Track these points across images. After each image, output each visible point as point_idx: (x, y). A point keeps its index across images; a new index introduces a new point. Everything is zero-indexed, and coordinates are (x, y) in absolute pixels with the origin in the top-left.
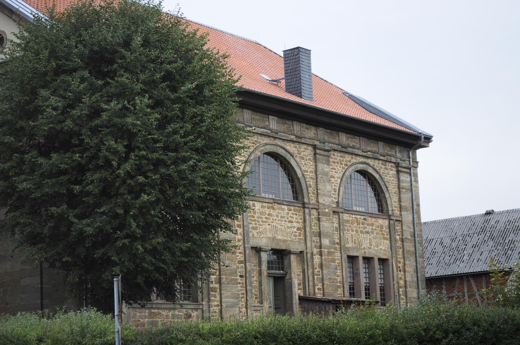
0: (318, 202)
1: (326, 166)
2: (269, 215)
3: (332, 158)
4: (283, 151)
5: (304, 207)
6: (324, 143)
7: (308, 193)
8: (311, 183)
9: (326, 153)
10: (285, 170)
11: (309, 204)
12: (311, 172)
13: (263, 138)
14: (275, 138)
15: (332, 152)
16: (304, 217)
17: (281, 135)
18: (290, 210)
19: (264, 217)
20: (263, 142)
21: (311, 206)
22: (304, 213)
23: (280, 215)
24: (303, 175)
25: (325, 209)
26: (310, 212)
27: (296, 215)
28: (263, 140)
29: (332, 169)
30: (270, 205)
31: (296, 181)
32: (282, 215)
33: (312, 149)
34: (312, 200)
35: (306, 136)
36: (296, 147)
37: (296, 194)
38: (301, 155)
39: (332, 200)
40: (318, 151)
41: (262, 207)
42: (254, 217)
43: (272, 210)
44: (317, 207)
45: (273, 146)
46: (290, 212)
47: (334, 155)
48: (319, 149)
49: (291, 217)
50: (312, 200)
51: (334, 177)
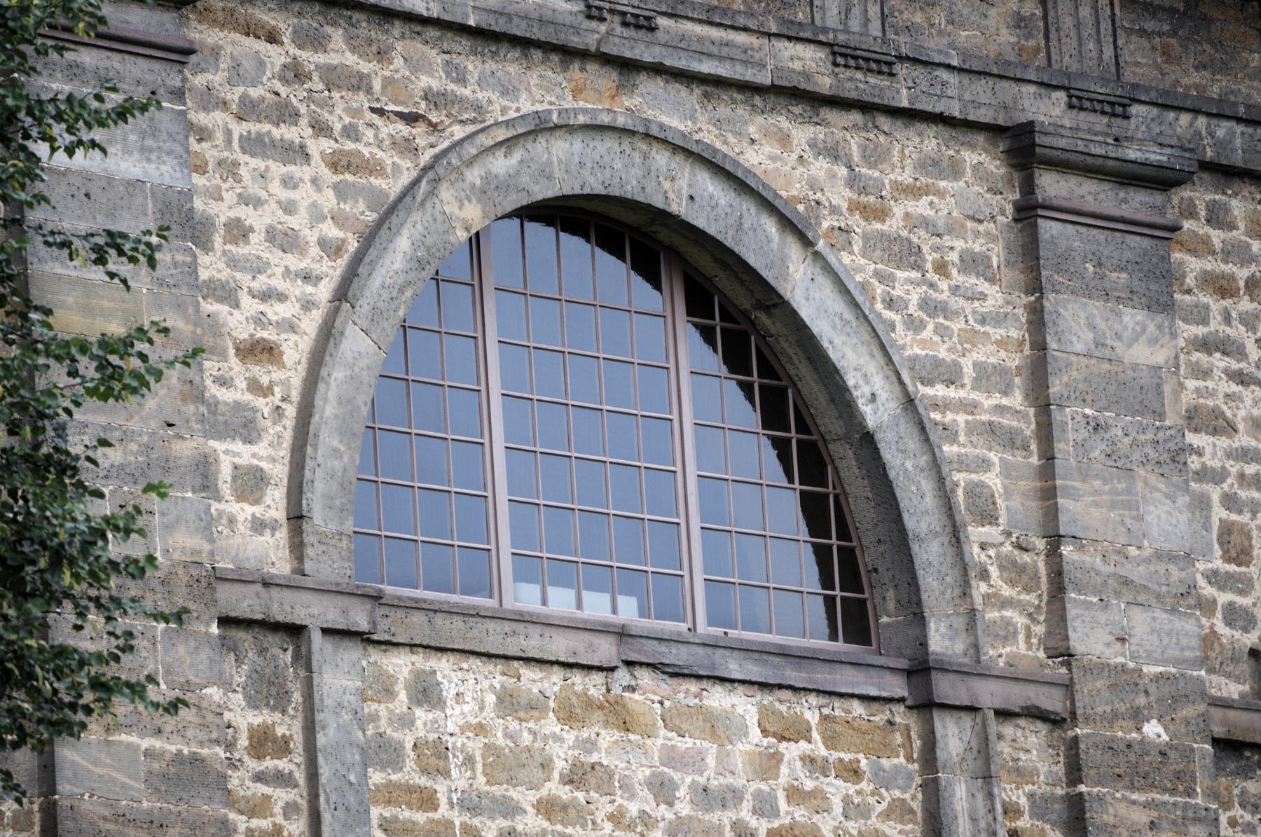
0: (1065, 655)
1: (1132, 317)
2: (574, 778)
3: (1202, 247)
4: (709, 185)
5: (926, 706)
6: (1117, 108)
7: (964, 571)
8: (994, 480)
9: (1137, 203)
10: (736, 360)
11: (977, 670)
12: (987, 377)
13: (510, 66)
14: (627, 67)
15: (1201, 195)
16: (933, 791)
17: (679, 45)
18: (794, 731)
19: (525, 797)
20: (500, 108)
21: (990, 694)
22: (929, 758)
23: (685, 782)
24: (909, 402)
25: (1138, 717)
26: (984, 748)
27: (854, 773)
28: (508, 91)
29: (1206, 345)
30: (593, 685)
31: (846, 461)
32: (711, 776)
33: (995, 166)
34: (1007, 634)
35: (934, 47)
36: (834, 153)
37: (852, 579)
38: (893, 225)
39: (1210, 639)
40: (1051, 185)
41: (509, 703)
42: (428, 801)
43: (608, 737)
44: (1052, 701)
45: (604, 147)
46: (792, 751)
47: (1217, 217)
48: (1062, 165)
49: (795, 794)
50: (1007, 634)
51: (1220, 425)
